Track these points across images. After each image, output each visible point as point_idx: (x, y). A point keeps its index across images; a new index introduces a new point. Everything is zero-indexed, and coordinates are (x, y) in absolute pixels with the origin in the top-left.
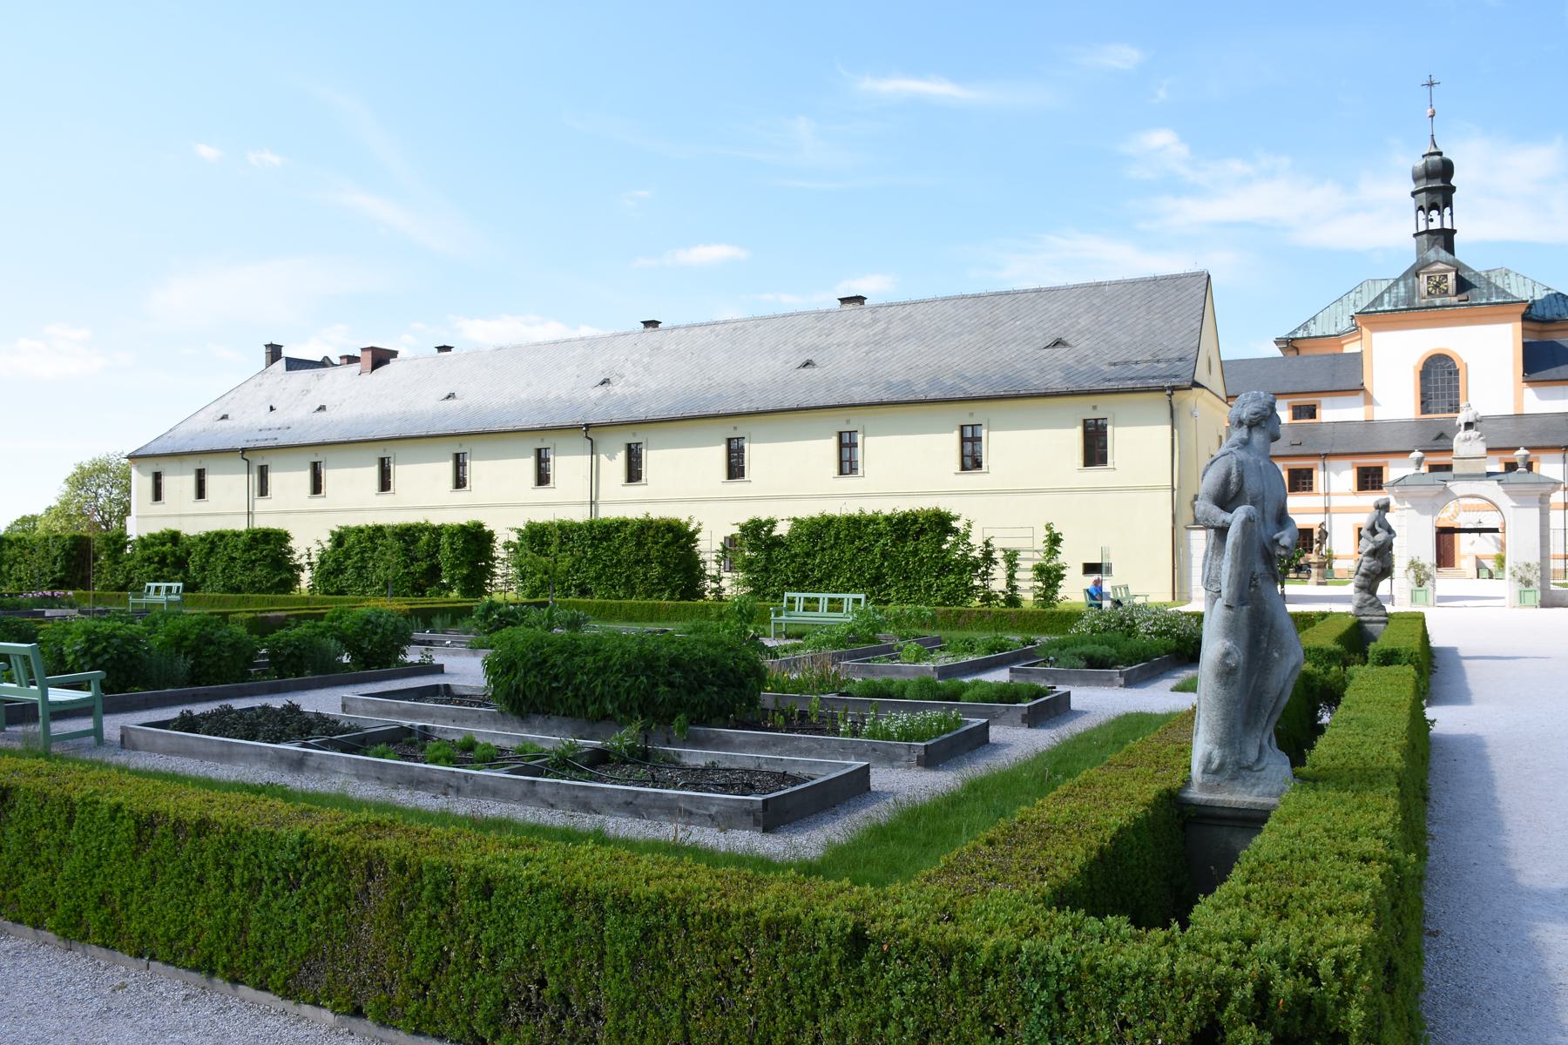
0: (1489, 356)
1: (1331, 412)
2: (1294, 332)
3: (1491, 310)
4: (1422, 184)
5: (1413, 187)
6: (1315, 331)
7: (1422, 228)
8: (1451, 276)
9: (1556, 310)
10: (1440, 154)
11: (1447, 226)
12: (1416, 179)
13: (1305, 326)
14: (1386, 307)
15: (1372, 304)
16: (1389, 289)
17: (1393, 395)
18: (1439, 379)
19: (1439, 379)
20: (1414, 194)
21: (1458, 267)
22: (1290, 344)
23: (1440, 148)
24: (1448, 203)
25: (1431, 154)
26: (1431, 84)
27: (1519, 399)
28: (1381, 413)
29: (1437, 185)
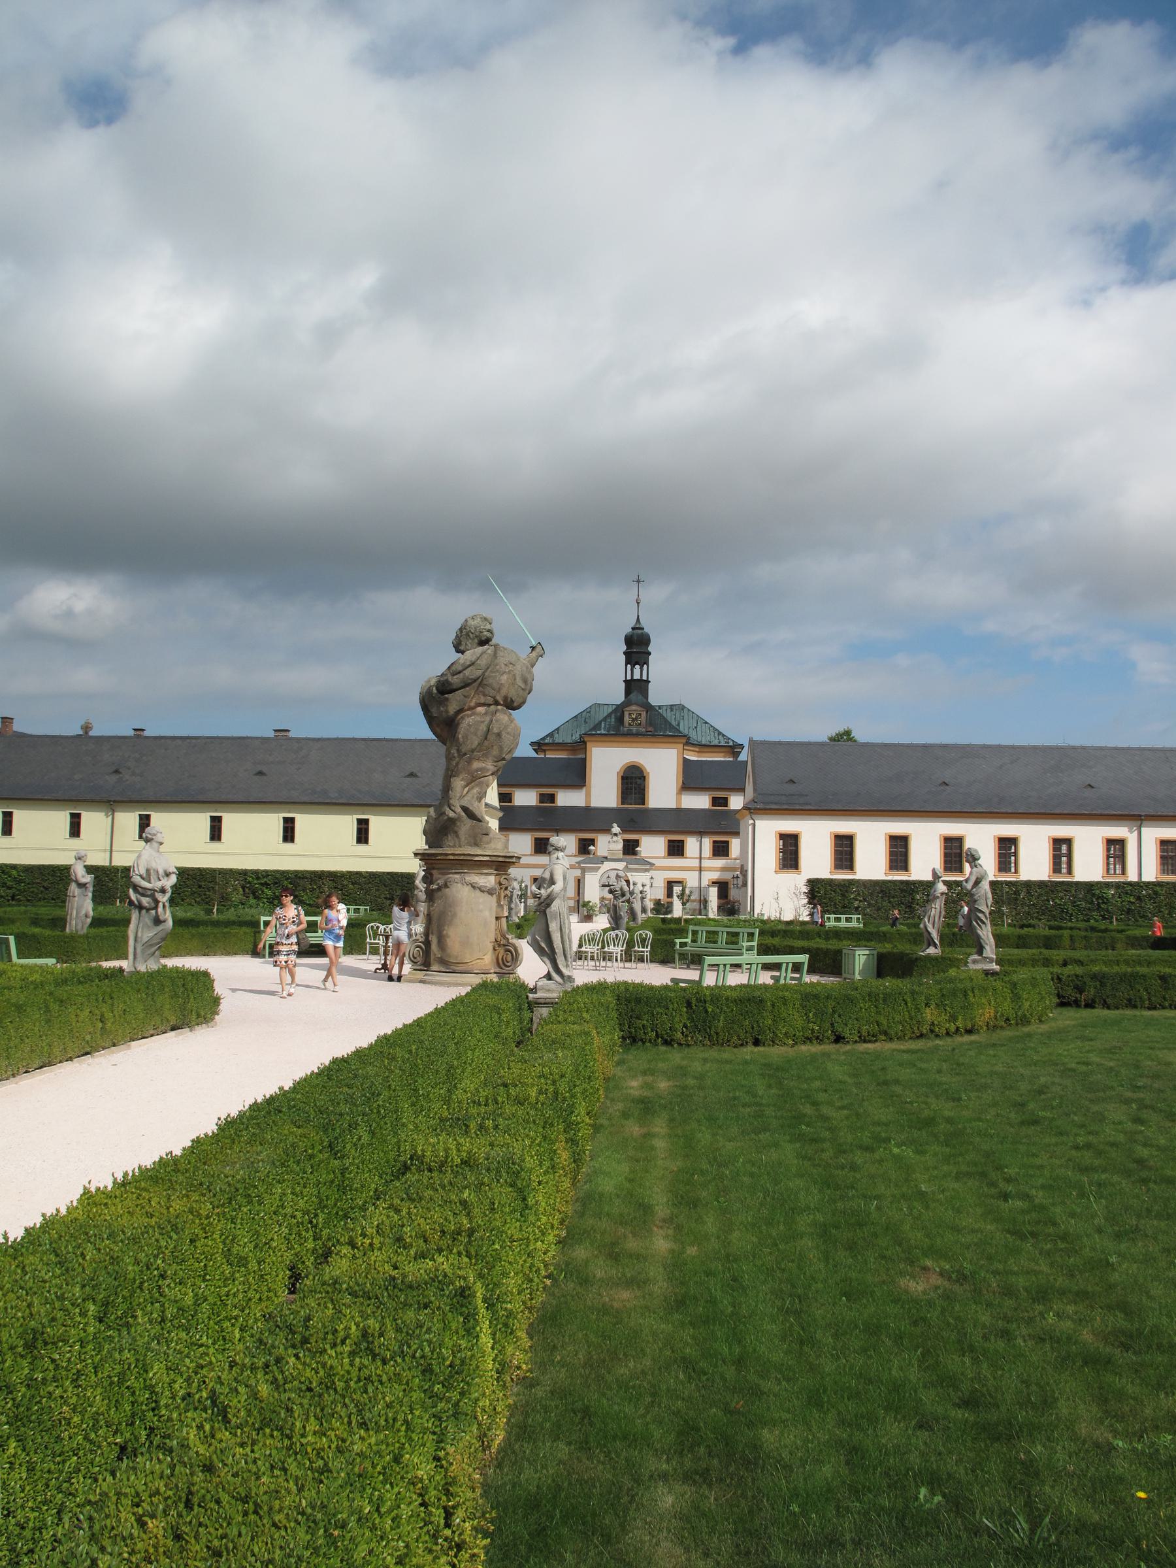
0: (663, 768)
1: (567, 799)
2: (543, 739)
3: (666, 739)
6: (558, 739)
7: (629, 678)
11: (645, 678)
13: (551, 735)
14: (603, 732)
15: (594, 728)
16: (605, 719)
17: (602, 790)
18: (633, 782)
19: (633, 782)
21: (649, 708)
22: (539, 746)
24: (646, 663)
26: (638, 581)
27: (679, 801)
29: (637, 648)
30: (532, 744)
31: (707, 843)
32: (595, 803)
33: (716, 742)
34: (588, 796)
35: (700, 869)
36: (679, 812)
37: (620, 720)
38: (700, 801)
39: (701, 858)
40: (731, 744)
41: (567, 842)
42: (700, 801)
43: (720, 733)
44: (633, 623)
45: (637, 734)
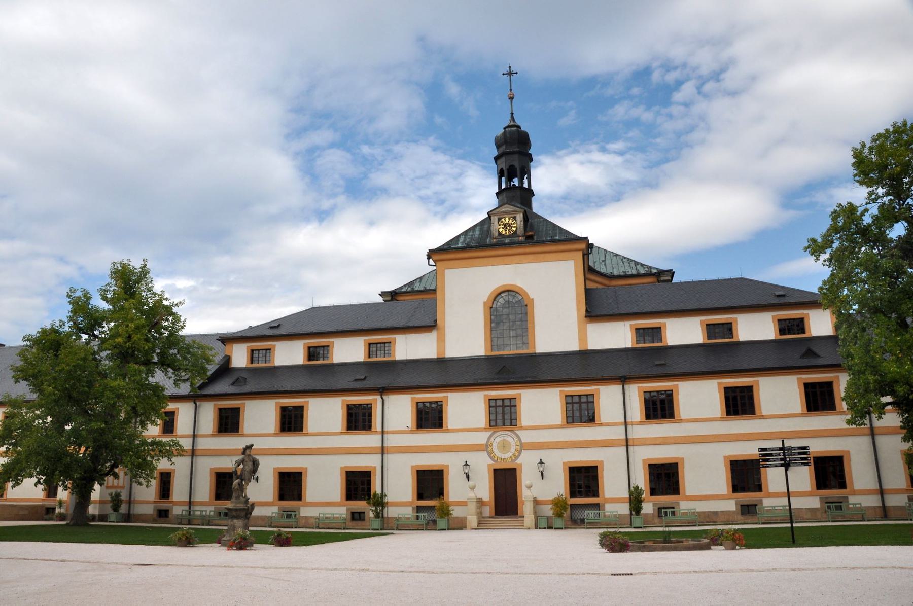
2: (401, 288)
4: (503, 149)
5: (496, 153)
6: (418, 287)
8: (520, 217)
9: (622, 269)
10: (519, 127)
12: (498, 146)
13: (411, 284)
14: (460, 245)
20: (496, 159)
22: (392, 296)
23: (518, 122)
25: (509, 126)
27: (583, 336)
28: (453, 351)
30: (383, 294)
31: (635, 393)
32: (450, 353)
33: (634, 272)
34: (441, 340)
35: (627, 443)
36: (585, 355)
37: (488, 232)
38: (616, 336)
39: (626, 424)
40: (654, 271)
41: (398, 410)
42: (616, 336)
43: (636, 263)
44: (507, 122)
45: (511, 245)
